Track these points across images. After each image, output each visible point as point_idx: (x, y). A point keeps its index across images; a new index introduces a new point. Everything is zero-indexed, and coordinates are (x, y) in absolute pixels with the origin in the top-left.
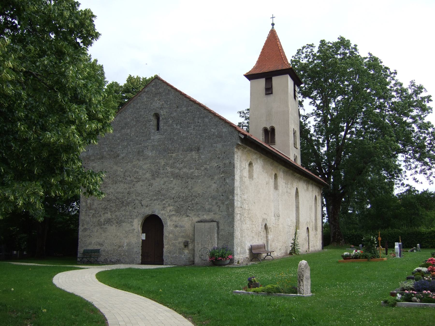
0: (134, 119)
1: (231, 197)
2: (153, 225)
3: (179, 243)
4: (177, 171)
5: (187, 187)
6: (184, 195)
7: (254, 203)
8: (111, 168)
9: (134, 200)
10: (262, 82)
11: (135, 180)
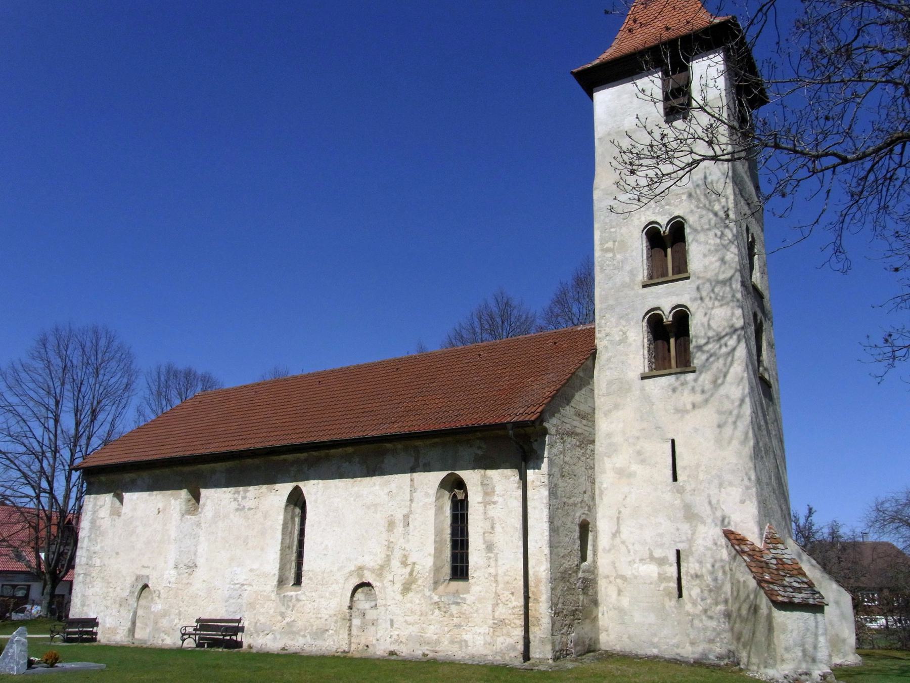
7: (117, 554)
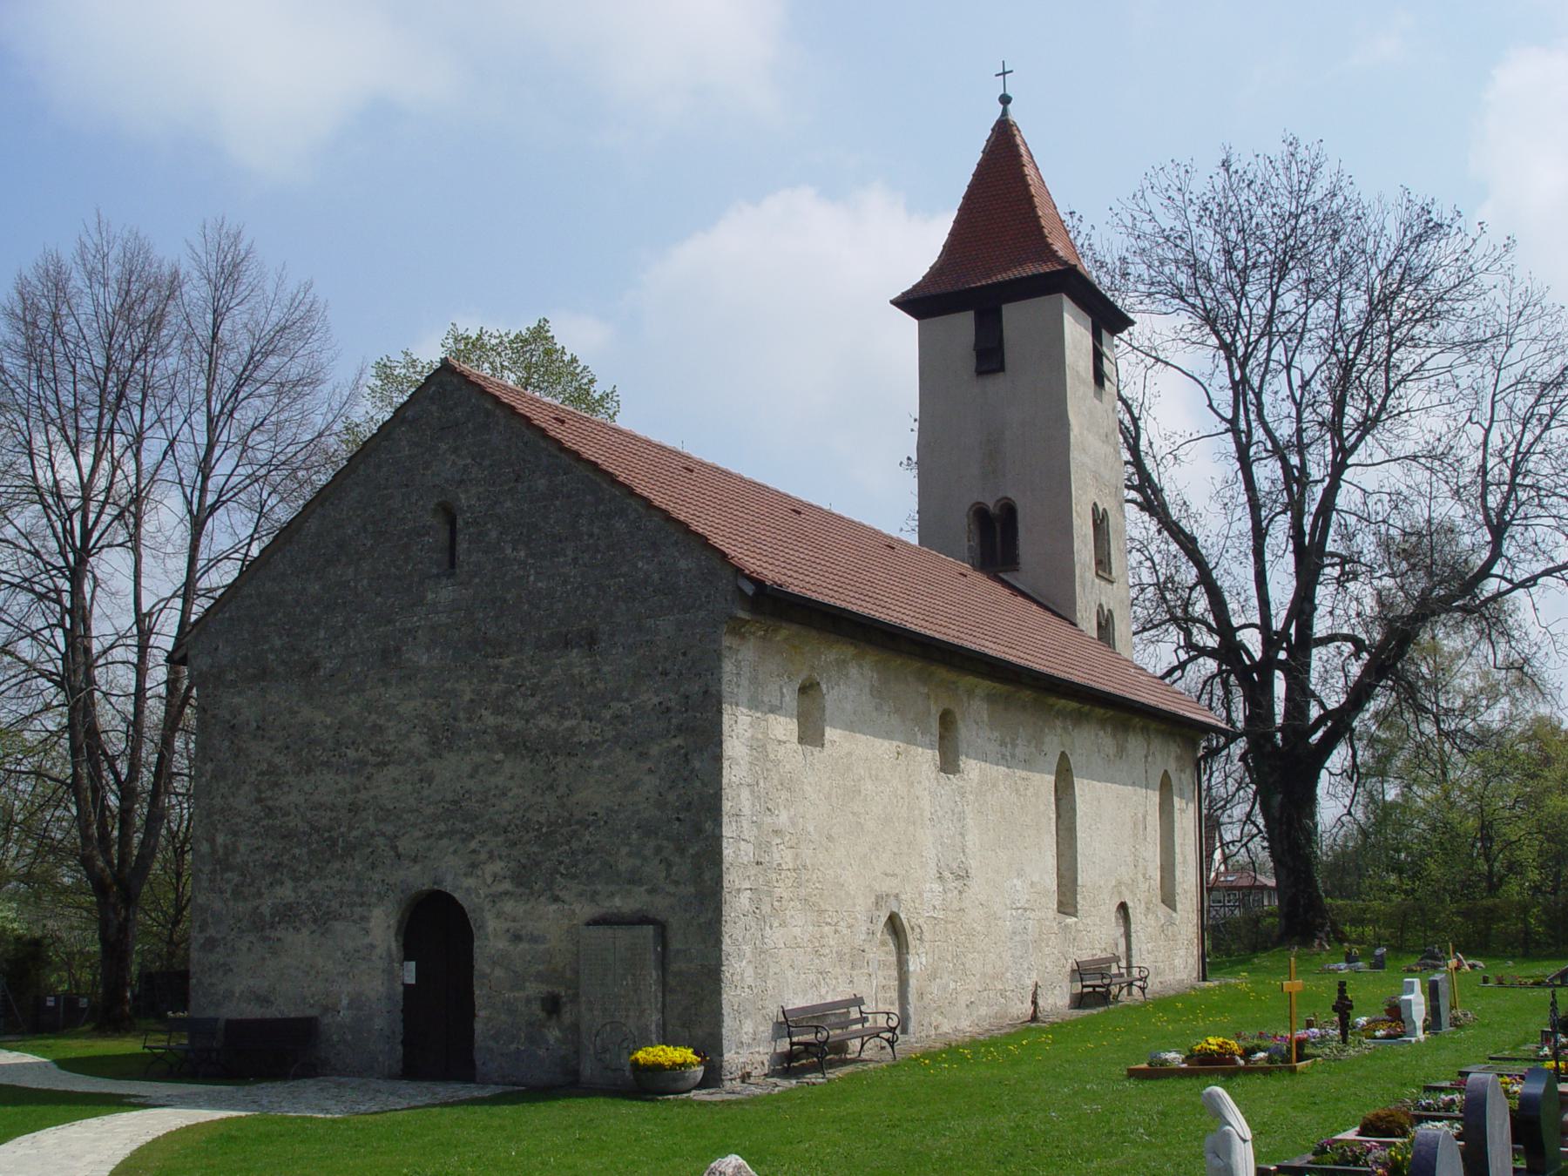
0: (370, 528)
1: (708, 826)
2: (436, 928)
3: (528, 1001)
4: (518, 724)
5: (551, 787)
6: (542, 819)
8: (294, 713)
9: (372, 835)
10: (963, 325)
11: (372, 759)
